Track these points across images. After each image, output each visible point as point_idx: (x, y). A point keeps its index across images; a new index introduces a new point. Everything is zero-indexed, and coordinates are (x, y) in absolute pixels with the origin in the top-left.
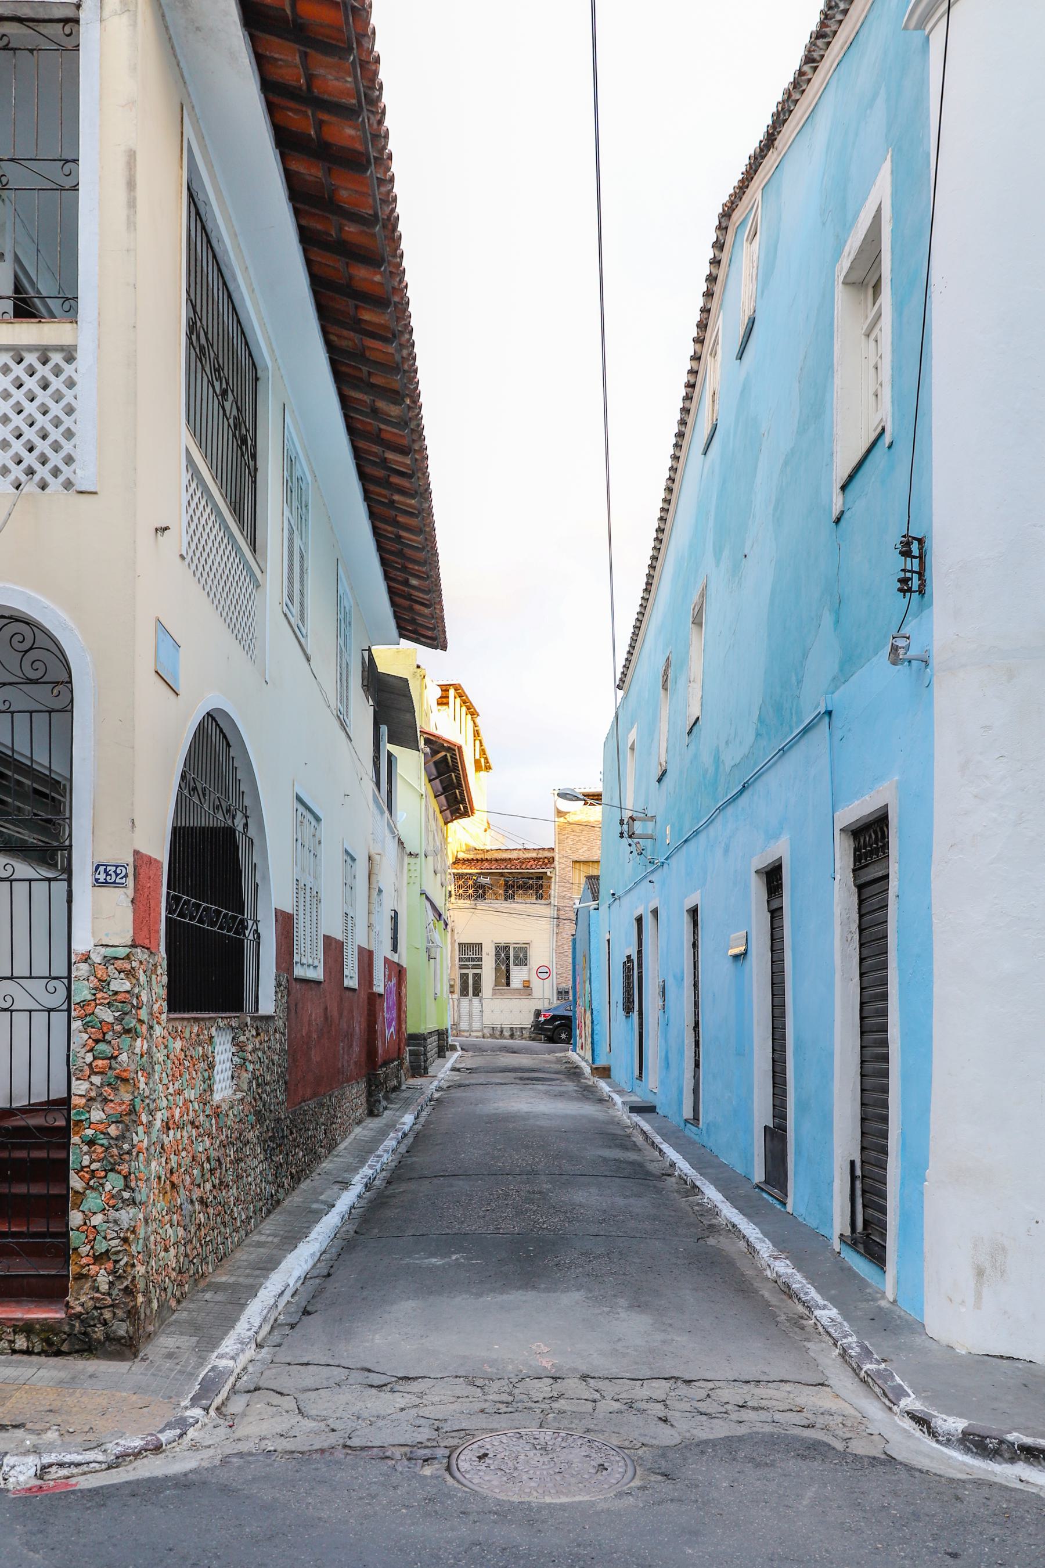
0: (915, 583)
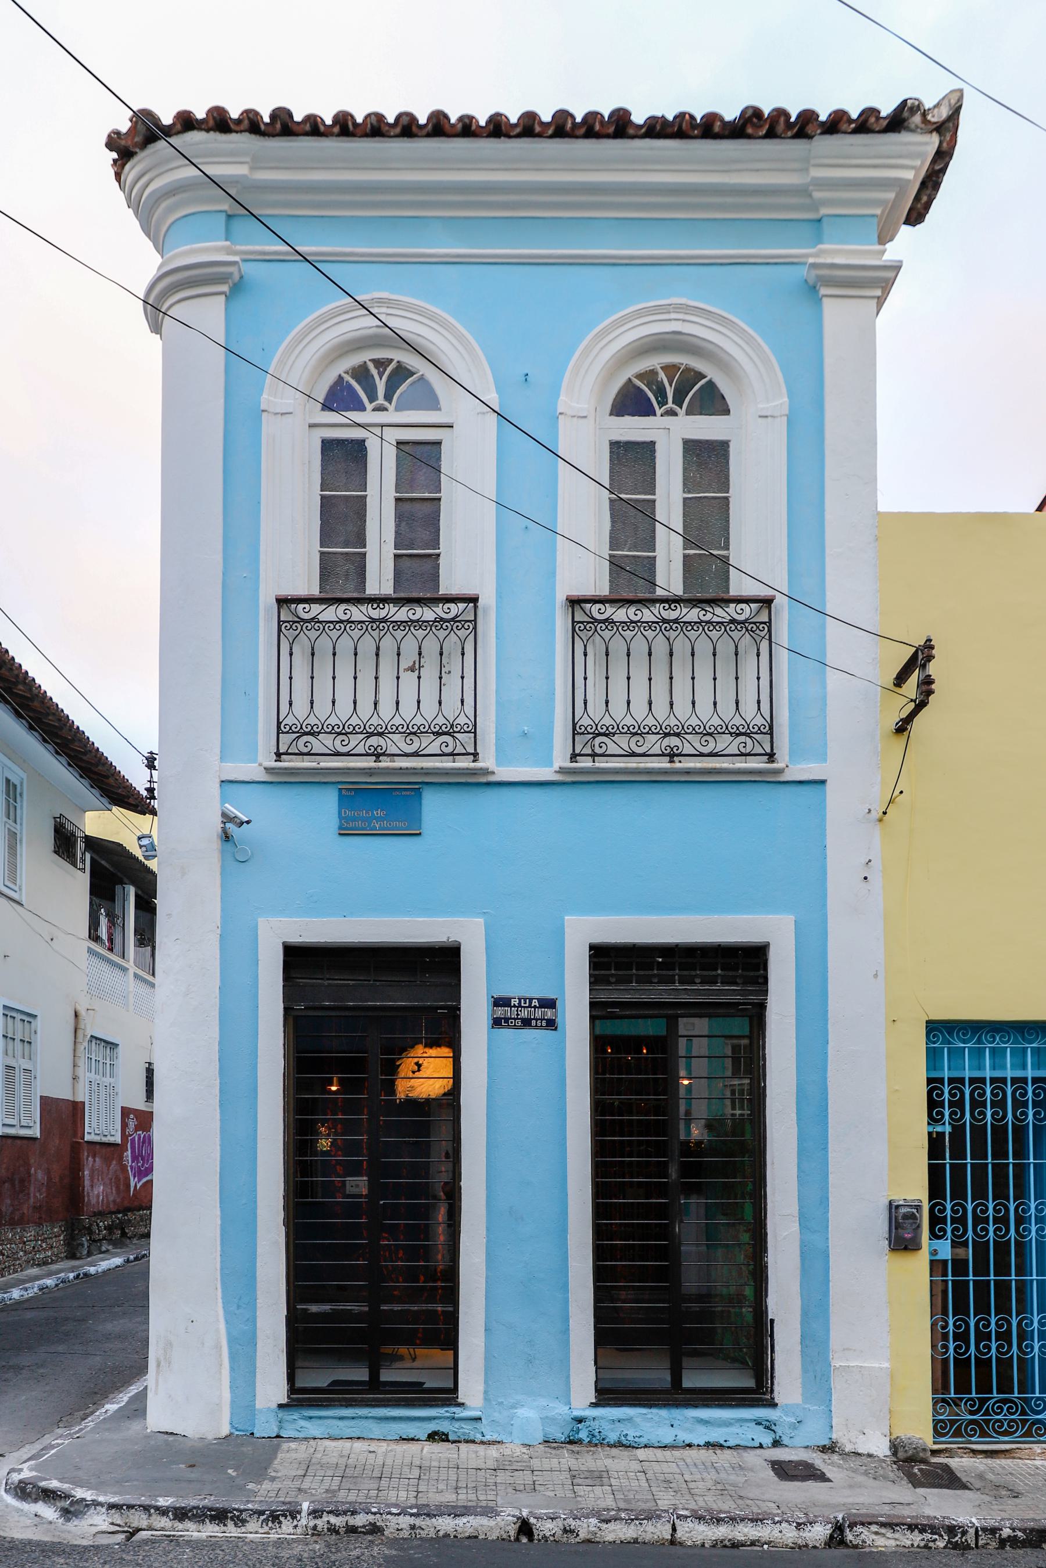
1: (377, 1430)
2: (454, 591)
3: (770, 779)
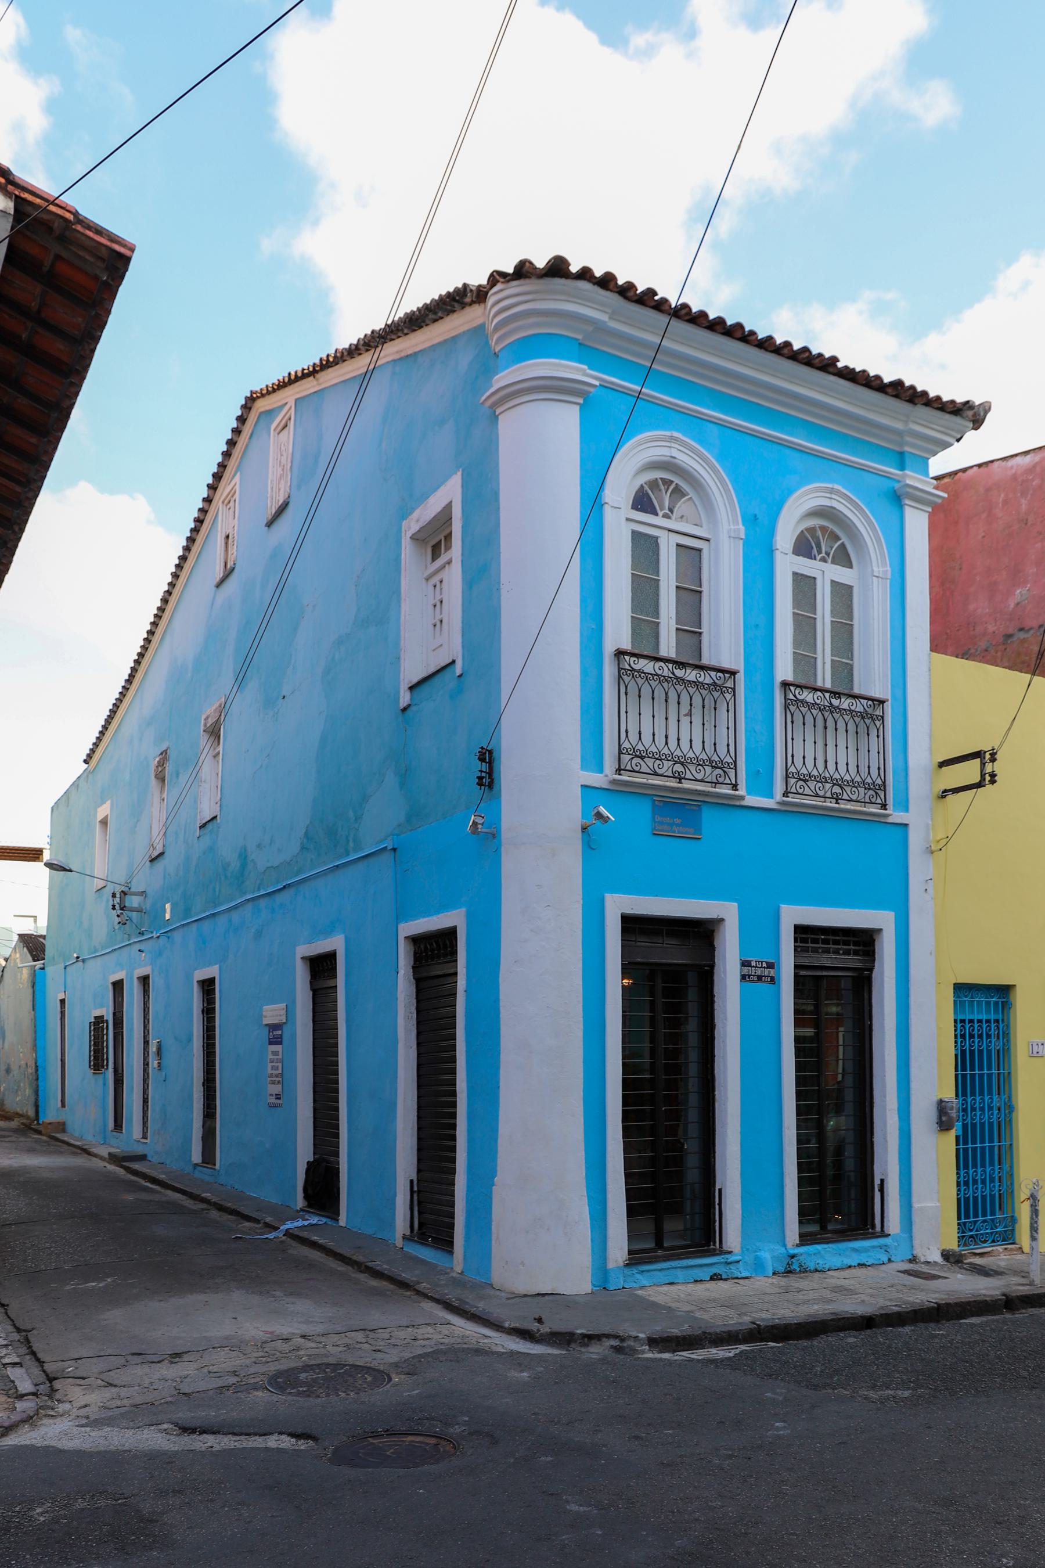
0: (486, 781)
1: (680, 1275)
2: (713, 663)
3: (880, 821)
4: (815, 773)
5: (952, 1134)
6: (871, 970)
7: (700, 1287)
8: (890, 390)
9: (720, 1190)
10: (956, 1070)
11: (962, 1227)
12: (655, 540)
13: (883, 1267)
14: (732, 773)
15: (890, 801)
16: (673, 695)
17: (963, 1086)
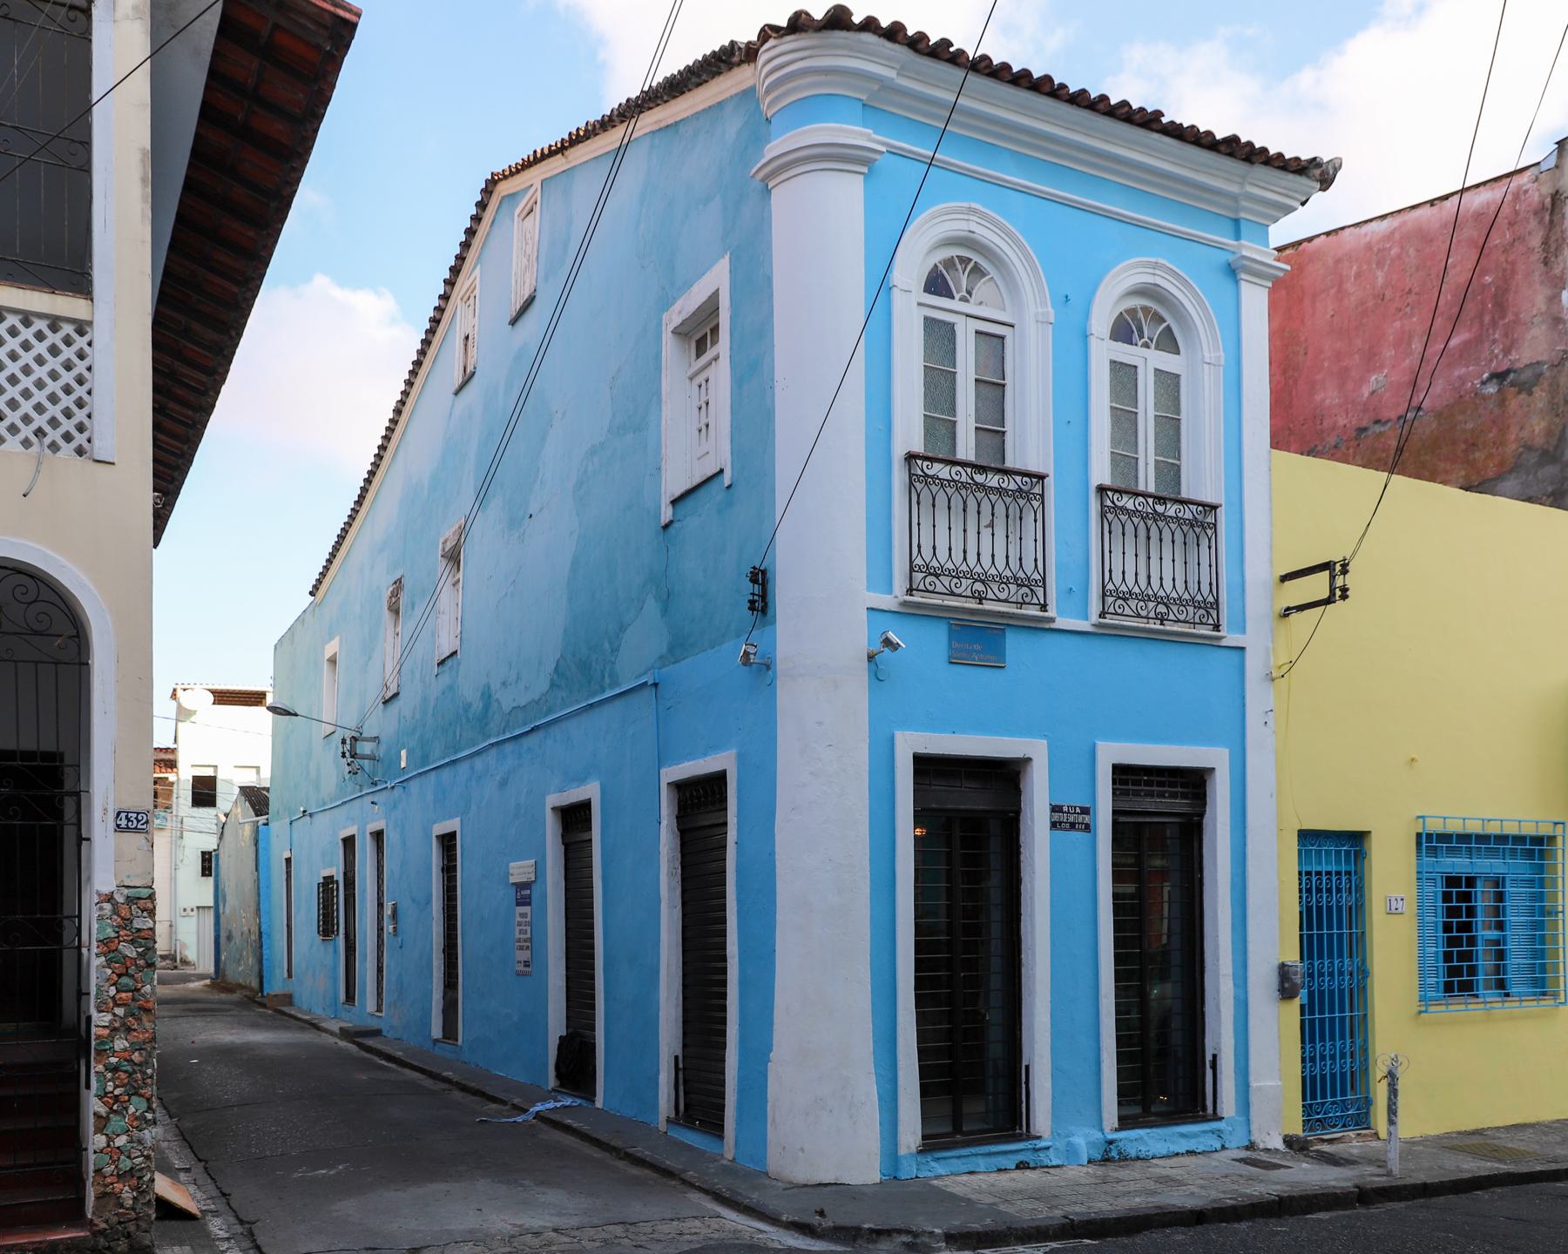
1: (982, 1163)
2: (1018, 466)
4: (1136, 590)
5: (1297, 1002)
6: (1202, 815)
7: (1004, 1177)
8: (1222, 148)
9: (1027, 1067)
10: (1301, 929)
11: (1307, 1110)
12: (950, 328)
13: (1216, 1155)
14: (1040, 592)
15: (1224, 621)
16: (972, 503)
17: (1308, 947)
